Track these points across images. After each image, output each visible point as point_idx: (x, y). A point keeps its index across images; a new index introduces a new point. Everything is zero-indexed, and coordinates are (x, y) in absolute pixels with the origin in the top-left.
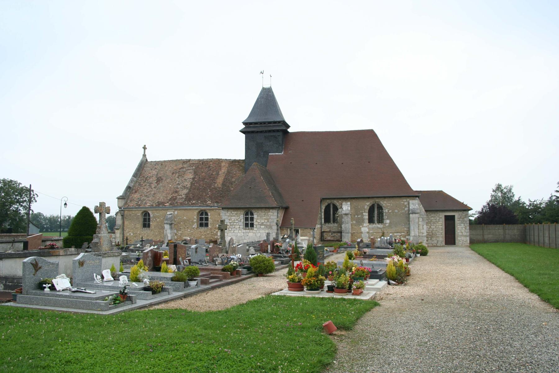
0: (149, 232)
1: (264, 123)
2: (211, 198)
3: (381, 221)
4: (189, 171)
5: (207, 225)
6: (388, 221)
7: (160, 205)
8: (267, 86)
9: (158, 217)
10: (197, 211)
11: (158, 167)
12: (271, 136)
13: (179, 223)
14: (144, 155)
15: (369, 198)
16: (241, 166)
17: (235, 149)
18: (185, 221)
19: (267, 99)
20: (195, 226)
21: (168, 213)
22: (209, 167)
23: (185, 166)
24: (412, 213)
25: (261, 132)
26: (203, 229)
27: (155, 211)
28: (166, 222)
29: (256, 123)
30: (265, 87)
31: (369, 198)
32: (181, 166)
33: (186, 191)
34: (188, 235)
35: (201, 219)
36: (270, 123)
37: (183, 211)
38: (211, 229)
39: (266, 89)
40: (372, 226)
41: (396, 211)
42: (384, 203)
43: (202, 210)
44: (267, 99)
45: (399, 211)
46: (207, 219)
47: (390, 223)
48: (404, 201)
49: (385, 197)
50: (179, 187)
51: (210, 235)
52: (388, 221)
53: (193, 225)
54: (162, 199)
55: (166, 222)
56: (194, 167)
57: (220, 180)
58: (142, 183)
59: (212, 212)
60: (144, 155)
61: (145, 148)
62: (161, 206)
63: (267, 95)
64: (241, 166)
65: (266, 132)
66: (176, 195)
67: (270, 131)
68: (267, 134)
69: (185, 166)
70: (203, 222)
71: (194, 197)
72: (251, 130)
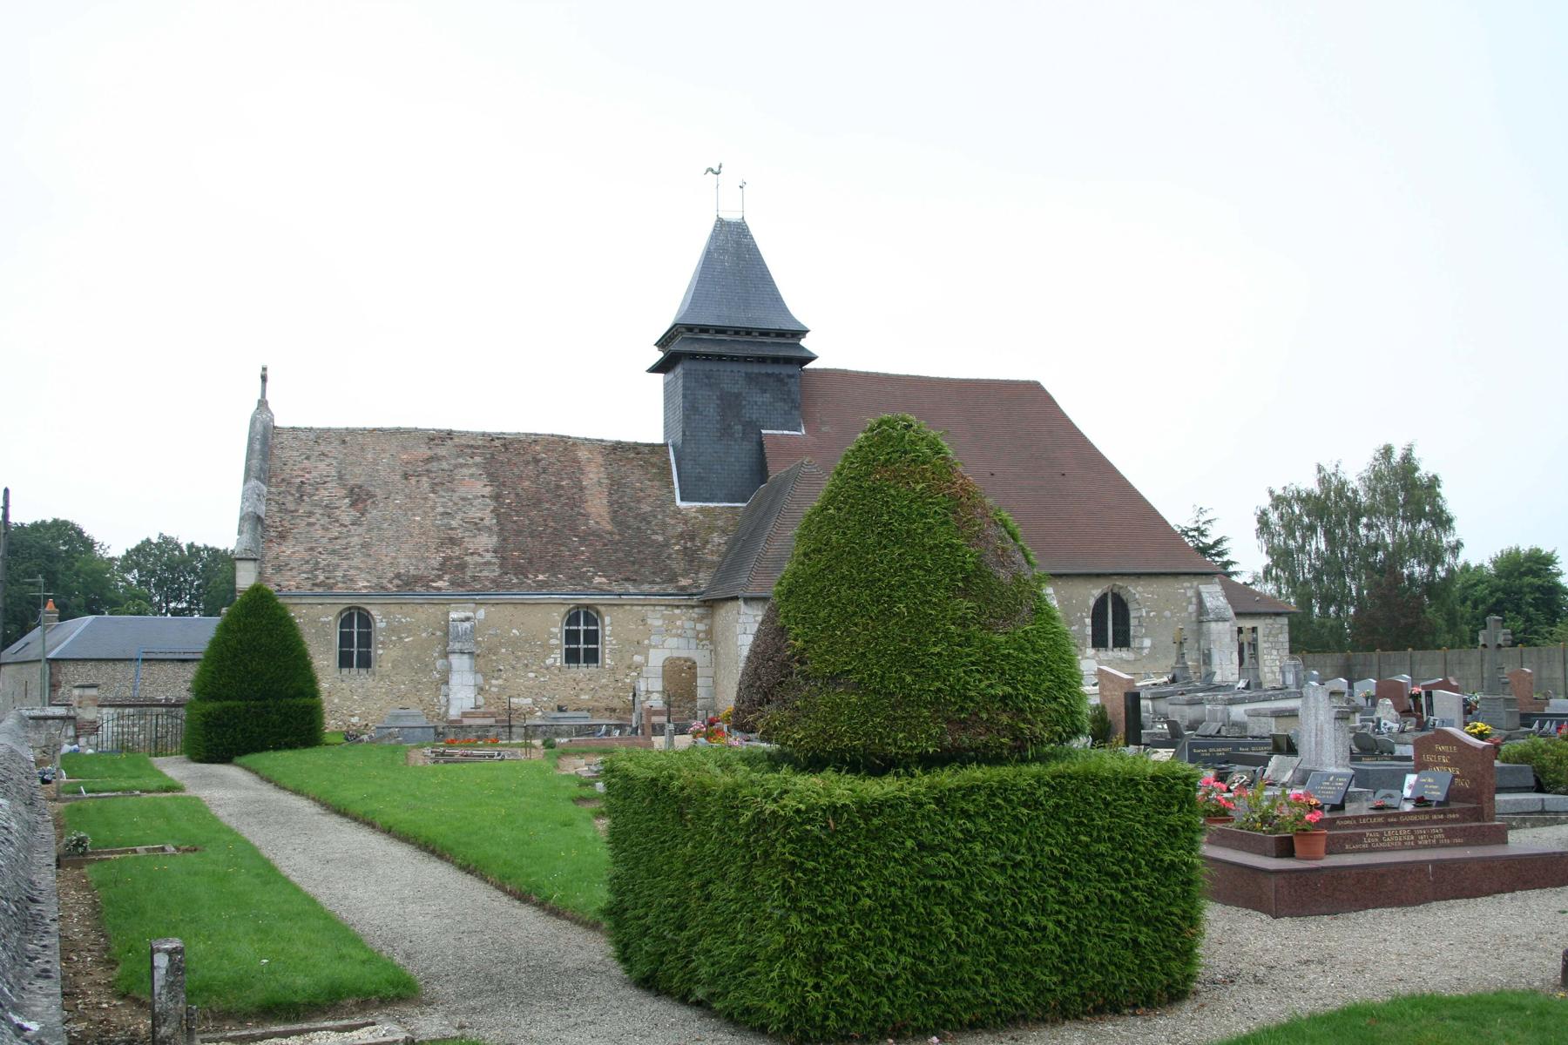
0: (370, 683)
1: (749, 332)
2: (1404, 519)
3: (1123, 640)
4: (465, 471)
5: (592, 657)
6: (1147, 643)
7: (409, 586)
8: (732, 216)
9: (409, 629)
10: (564, 610)
11: (333, 449)
12: (768, 375)
13: (493, 650)
14: (263, 403)
15: (1098, 575)
16: (653, 465)
17: (631, 406)
18: (514, 644)
19: (733, 257)
20: (557, 658)
21: (453, 615)
22: (537, 461)
23: (442, 451)
24: (1217, 621)
25: (733, 359)
26: (582, 670)
27: (392, 608)
28: (457, 646)
29: (721, 330)
30: (727, 216)
31: (1098, 575)
32: (424, 451)
33: (487, 541)
34: (529, 691)
35: (571, 636)
36: (765, 333)
37: (511, 608)
38: (613, 670)
39: (729, 224)
40: (1103, 654)
41: (1167, 613)
42: (1137, 592)
43: (578, 606)
44: (733, 257)
45: (1173, 614)
46: (592, 637)
47: (1153, 646)
48: (1186, 588)
49: (1139, 575)
50: (454, 523)
51: (610, 692)
52: (1147, 643)
53: (547, 656)
54: (406, 565)
55: (457, 646)
56: (478, 459)
57: (597, 508)
58: (291, 506)
59: (619, 613)
60: (263, 403)
61: (264, 369)
62: (418, 589)
63: (738, 243)
64: (653, 465)
65: (745, 359)
66: (458, 551)
67: (762, 360)
68: (755, 369)
69: (442, 451)
70: (582, 645)
71: (530, 562)
72: (682, 352)
